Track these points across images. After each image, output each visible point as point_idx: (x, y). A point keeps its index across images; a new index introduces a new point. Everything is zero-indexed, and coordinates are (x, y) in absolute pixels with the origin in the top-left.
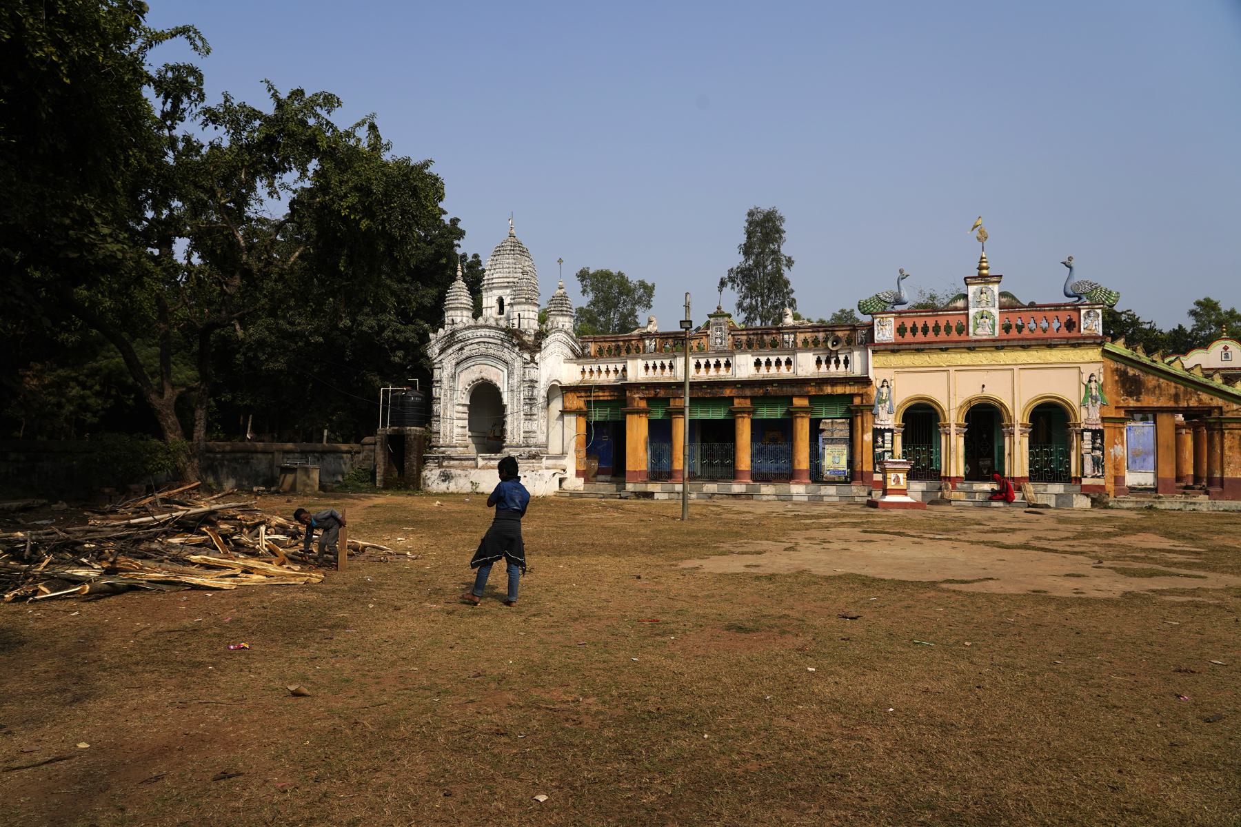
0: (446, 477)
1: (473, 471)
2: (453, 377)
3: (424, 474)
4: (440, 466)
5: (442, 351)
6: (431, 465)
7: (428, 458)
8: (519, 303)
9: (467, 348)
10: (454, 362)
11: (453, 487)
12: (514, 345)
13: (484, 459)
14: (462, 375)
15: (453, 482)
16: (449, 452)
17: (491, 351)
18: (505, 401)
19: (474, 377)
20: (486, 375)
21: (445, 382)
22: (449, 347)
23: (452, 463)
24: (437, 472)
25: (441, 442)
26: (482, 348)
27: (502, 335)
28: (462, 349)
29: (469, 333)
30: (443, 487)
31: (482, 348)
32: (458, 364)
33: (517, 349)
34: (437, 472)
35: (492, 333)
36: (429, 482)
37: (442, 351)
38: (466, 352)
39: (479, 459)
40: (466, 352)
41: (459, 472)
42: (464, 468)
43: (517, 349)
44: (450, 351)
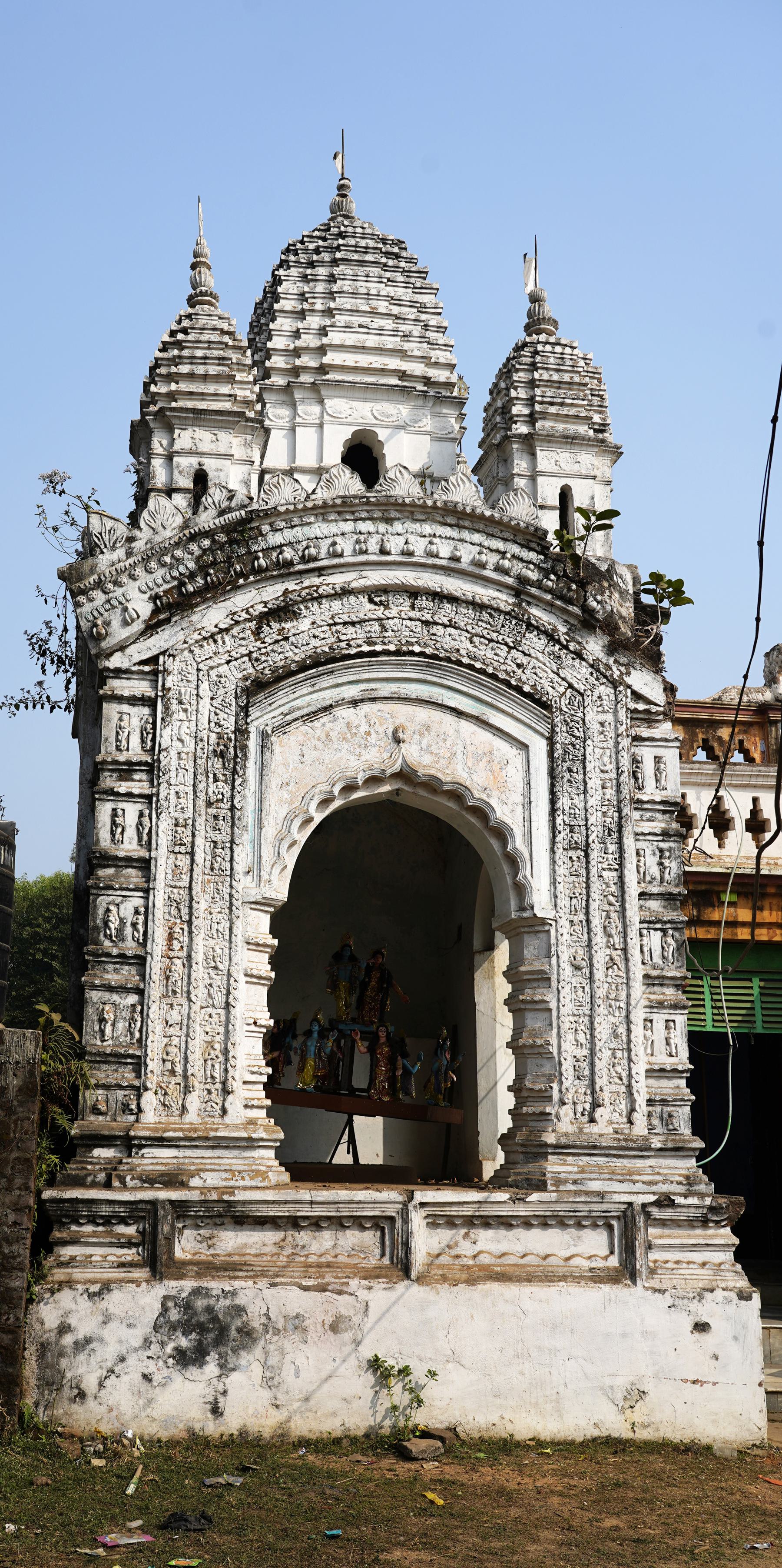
0: (206, 1335)
1: (379, 1296)
2: (230, 754)
3: (48, 1314)
4: (156, 1262)
5: (171, 607)
6: (91, 1254)
7: (88, 1212)
8: (570, 441)
9: (321, 612)
10: (232, 677)
11: (247, 1399)
12: (589, 622)
13: (433, 1222)
14: (284, 749)
15: (250, 1367)
16: (212, 1175)
17: (450, 641)
18: (541, 902)
19: (376, 756)
20: (420, 756)
21: (178, 778)
22: (213, 592)
23: (231, 1241)
24: (142, 1301)
25: (151, 1114)
26: (402, 622)
27: (526, 564)
28: (283, 611)
29: (339, 534)
30: (177, 1402)
31: (402, 622)
32: (257, 688)
33: (595, 646)
34: (142, 1301)
35: (469, 548)
36: (85, 1370)
37: (171, 607)
38: (308, 631)
39: (417, 1220)
40: (308, 631)
41: (289, 1299)
42: (323, 1277)
43: (595, 646)
44: (213, 615)
